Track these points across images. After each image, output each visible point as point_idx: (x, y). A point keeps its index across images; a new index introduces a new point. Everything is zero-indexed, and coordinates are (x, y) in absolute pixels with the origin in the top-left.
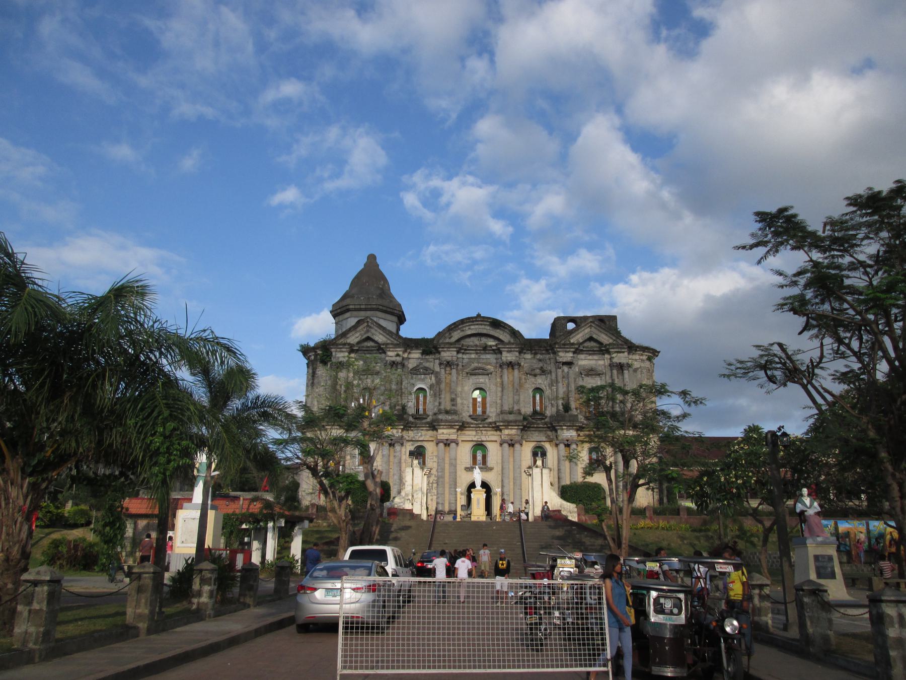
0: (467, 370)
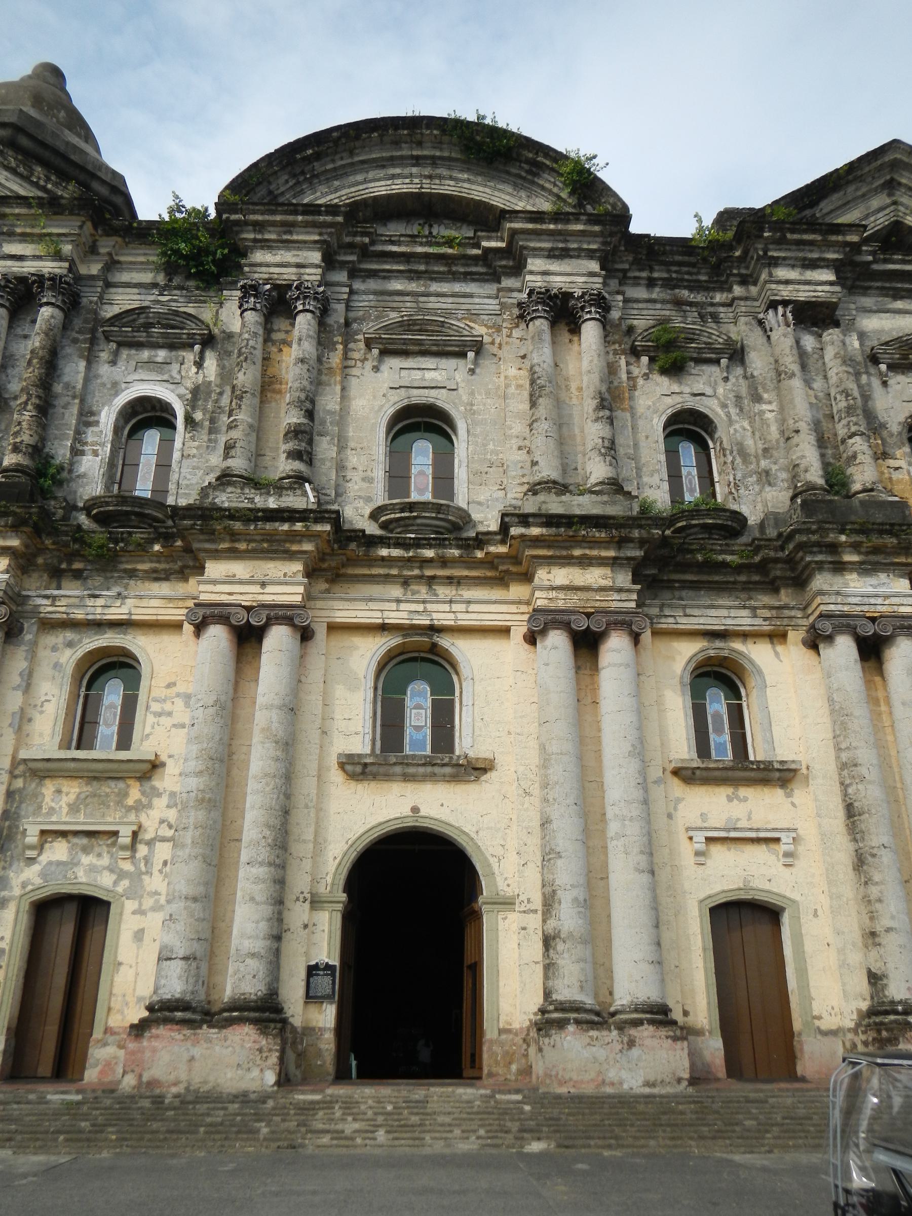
0: (369, 328)
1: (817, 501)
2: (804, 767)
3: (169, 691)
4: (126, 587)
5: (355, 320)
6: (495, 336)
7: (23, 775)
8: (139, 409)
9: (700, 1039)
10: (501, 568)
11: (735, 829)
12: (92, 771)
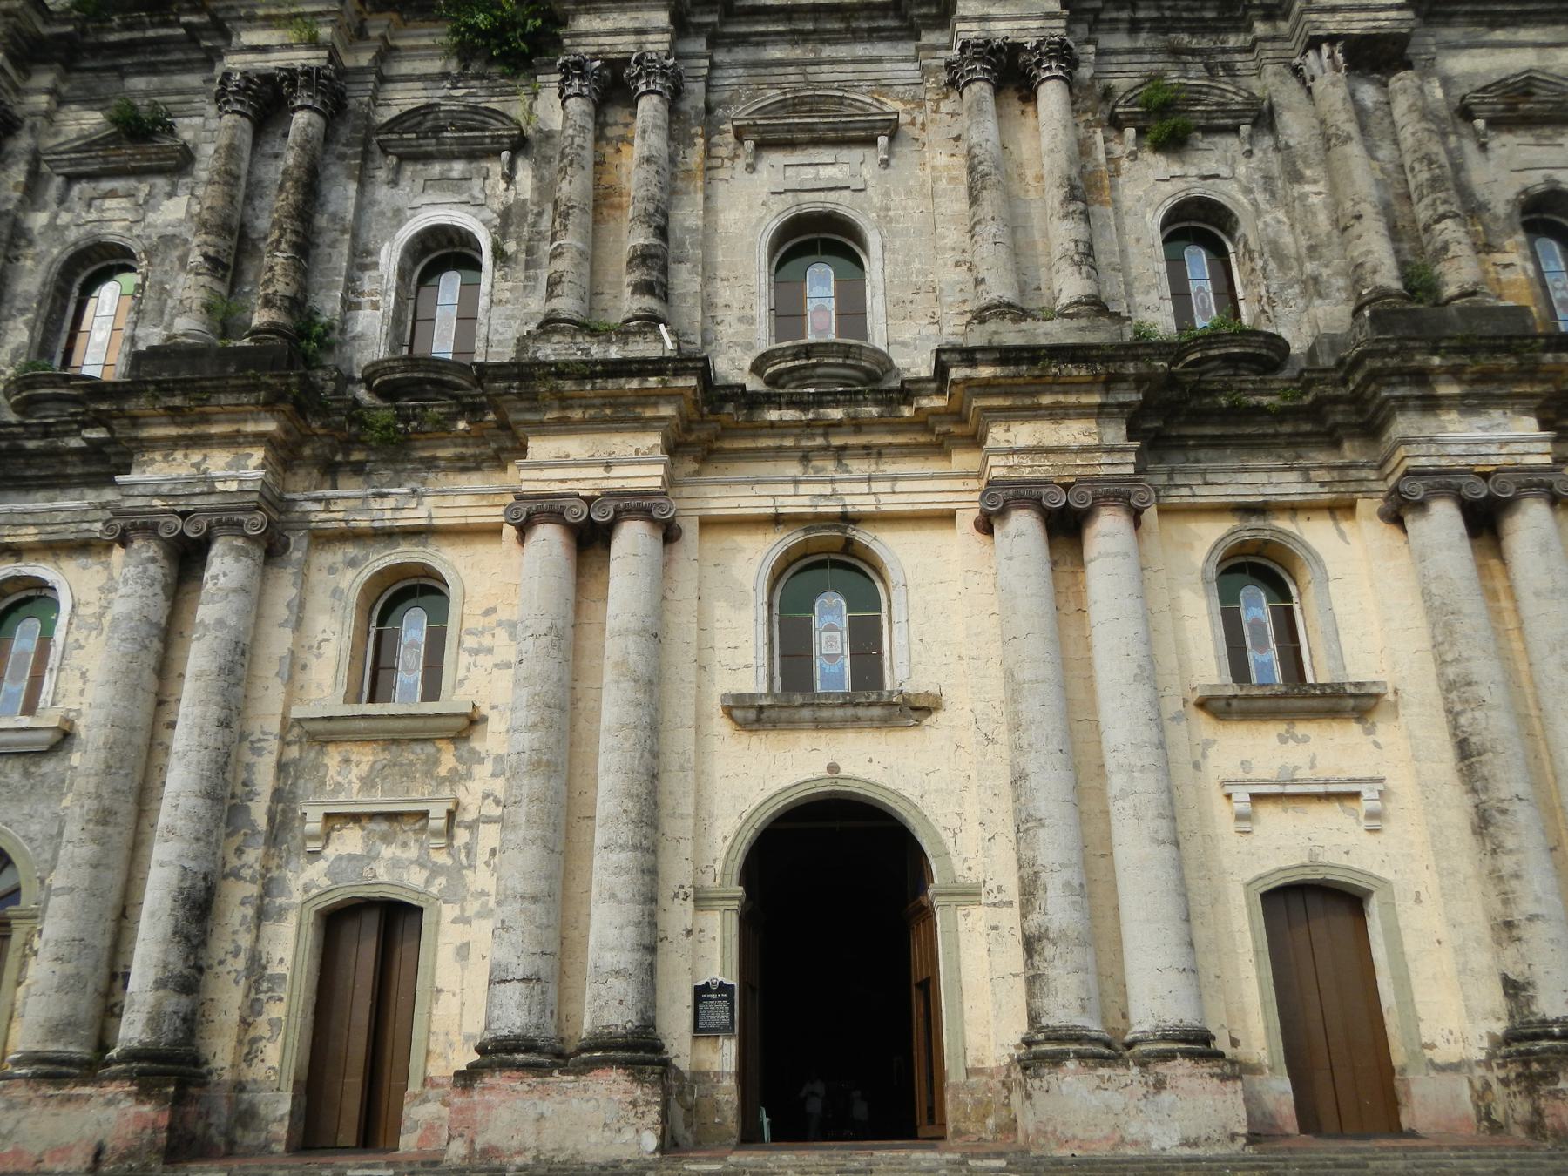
0: (740, 112)
1: (1394, 312)
2: (1390, 690)
3: (487, 619)
4: (424, 482)
5: (719, 104)
6: (915, 113)
7: (299, 741)
8: (432, 244)
9: (1257, 1078)
10: (938, 429)
11: (1293, 781)
12: (389, 732)
